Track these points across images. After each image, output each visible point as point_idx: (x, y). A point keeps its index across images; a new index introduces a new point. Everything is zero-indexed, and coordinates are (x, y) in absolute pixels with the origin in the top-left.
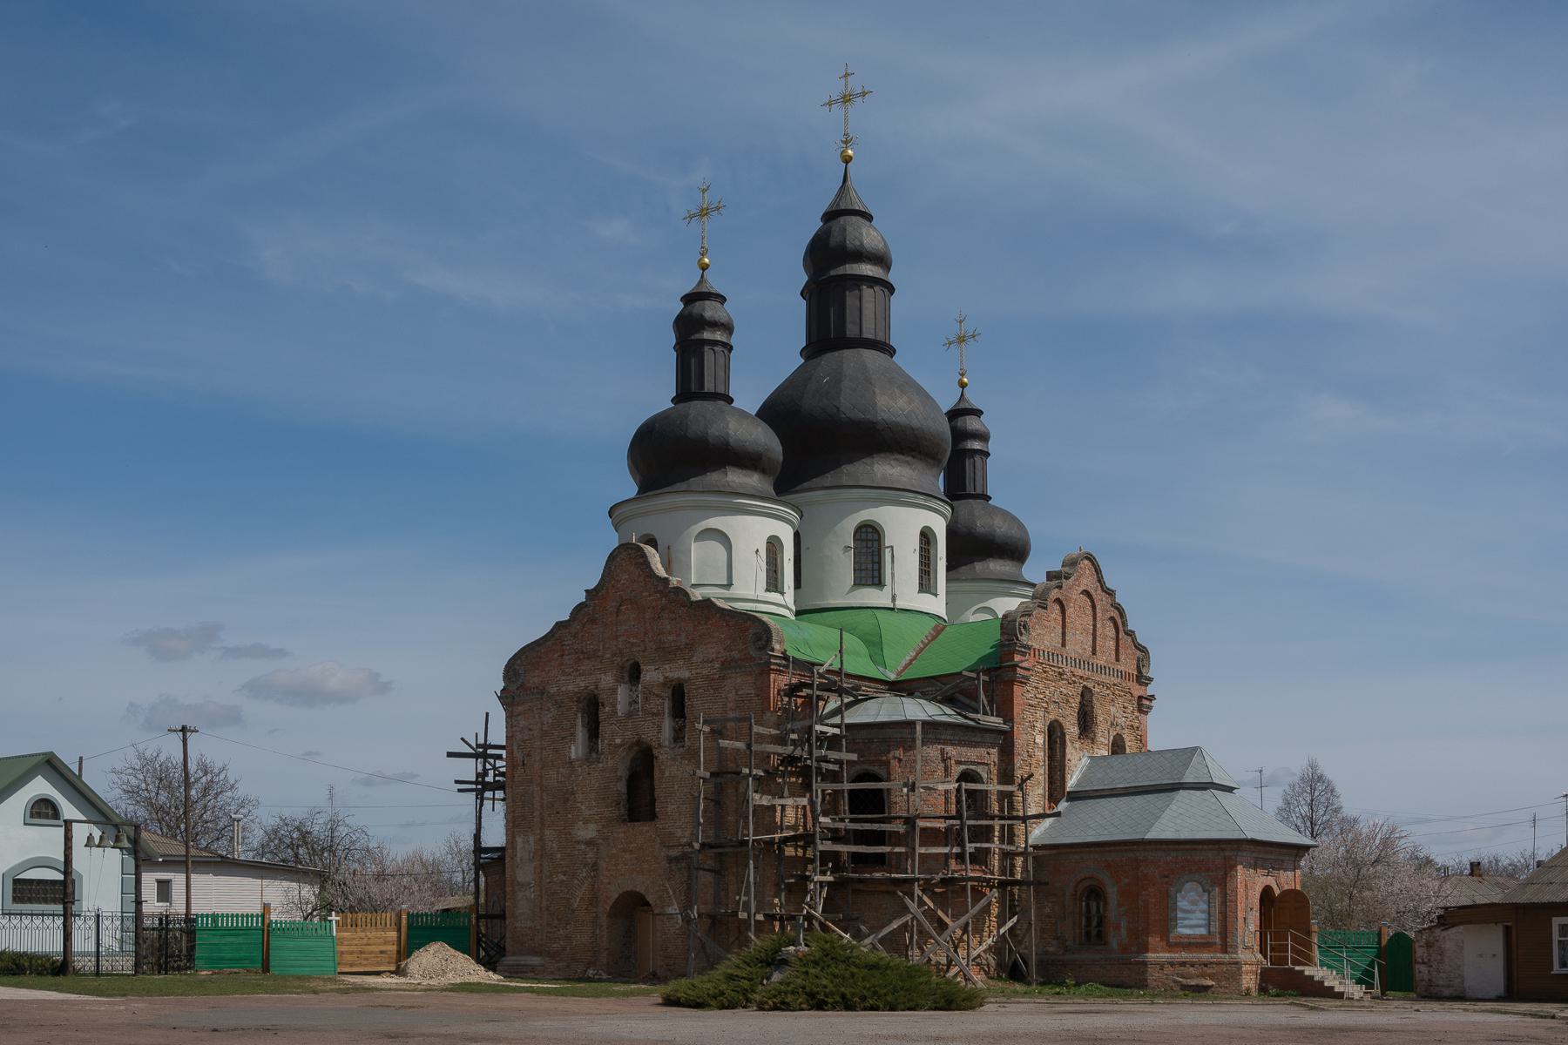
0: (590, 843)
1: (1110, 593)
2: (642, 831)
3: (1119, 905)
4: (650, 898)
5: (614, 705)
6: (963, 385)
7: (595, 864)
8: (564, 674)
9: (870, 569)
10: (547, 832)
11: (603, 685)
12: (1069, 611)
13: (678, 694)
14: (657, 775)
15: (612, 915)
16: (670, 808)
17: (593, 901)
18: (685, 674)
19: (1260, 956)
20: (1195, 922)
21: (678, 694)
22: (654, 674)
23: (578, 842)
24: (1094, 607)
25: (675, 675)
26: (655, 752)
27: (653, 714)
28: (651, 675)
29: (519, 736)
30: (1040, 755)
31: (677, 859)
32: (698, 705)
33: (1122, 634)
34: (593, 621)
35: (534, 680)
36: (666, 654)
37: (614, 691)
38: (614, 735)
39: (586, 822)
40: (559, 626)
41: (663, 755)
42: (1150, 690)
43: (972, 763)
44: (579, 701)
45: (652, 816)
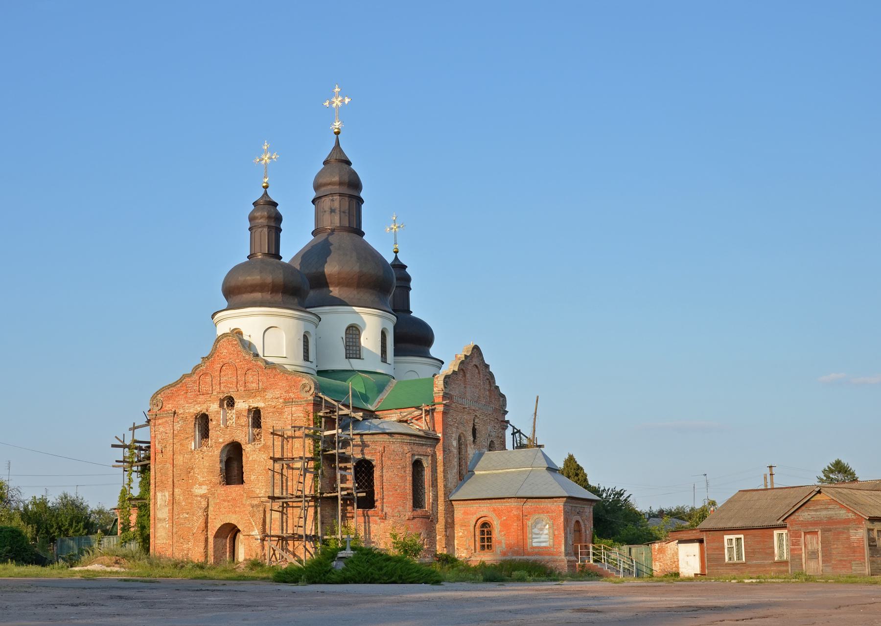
1: (487, 366)
3: (500, 531)
5: (218, 421)
6: (396, 252)
9: (353, 348)
10: (176, 490)
12: (468, 375)
13: (256, 416)
15: (216, 537)
16: (253, 477)
18: (260, 405)
19: (573, 558)
20: (541, 540)
21: (256, 416)
24: (479, 373)
26: (243, 447)
28: (241, 405)
29: (159, 437)
30: (455, 451)
31: (258, 506)
33: (493, 388)
34: (206, 374)
36: (250, 394)
37: (218, 413)
39: (201, 484)
41: (247, 449)
42: (507, 418)
43: (421, 455)
45: (242, 482)
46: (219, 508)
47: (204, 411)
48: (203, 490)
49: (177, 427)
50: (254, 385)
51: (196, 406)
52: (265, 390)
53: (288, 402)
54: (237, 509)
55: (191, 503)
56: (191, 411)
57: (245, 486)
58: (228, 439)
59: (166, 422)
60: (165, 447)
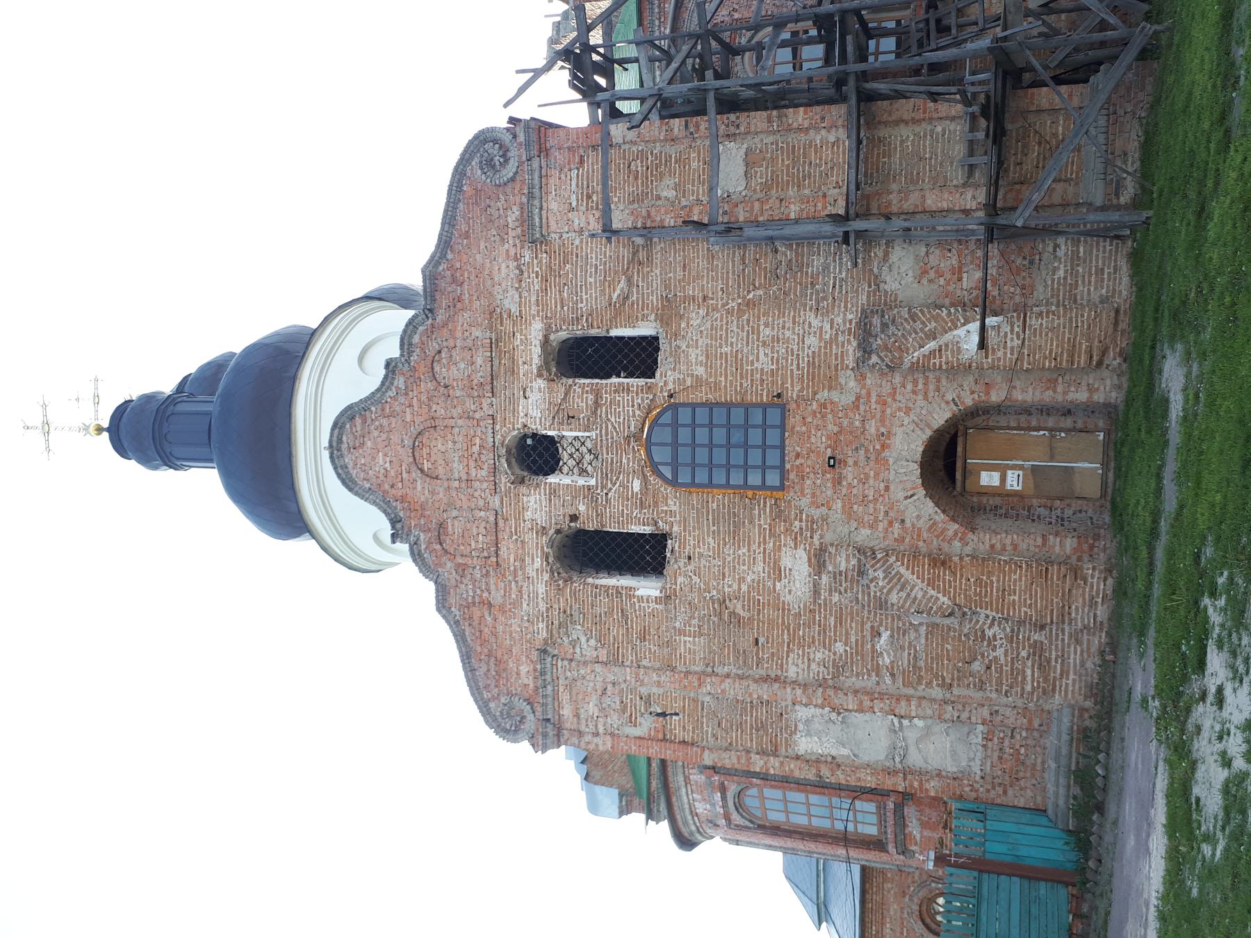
0: (819, 560)
2: (808, 439)
4: (940, 417)
5: (576, 492)
7: (860, 550)
8: (517, 604)
10: (792, 672)
11: (541, 519)
14: (702, 396)
16: (764, 361)
17: (940, 561)
18: (536, 329)
22: (534, 397)
23: (816, 592)
27: (597, 404)
28: (534, 406)
37: (553, 491)
39: (777, 572)
40: (443, 605)
44: (568, 580)
46: (864, 500)
48: (797, 562)
49: (588, 647)
52: (494, 315)
53: (534, 236)
54: (872, 428)
55: (840, 620)
56: (541, 589)
57: (793, 392)
59: (569, 687)
60: (648, 700)
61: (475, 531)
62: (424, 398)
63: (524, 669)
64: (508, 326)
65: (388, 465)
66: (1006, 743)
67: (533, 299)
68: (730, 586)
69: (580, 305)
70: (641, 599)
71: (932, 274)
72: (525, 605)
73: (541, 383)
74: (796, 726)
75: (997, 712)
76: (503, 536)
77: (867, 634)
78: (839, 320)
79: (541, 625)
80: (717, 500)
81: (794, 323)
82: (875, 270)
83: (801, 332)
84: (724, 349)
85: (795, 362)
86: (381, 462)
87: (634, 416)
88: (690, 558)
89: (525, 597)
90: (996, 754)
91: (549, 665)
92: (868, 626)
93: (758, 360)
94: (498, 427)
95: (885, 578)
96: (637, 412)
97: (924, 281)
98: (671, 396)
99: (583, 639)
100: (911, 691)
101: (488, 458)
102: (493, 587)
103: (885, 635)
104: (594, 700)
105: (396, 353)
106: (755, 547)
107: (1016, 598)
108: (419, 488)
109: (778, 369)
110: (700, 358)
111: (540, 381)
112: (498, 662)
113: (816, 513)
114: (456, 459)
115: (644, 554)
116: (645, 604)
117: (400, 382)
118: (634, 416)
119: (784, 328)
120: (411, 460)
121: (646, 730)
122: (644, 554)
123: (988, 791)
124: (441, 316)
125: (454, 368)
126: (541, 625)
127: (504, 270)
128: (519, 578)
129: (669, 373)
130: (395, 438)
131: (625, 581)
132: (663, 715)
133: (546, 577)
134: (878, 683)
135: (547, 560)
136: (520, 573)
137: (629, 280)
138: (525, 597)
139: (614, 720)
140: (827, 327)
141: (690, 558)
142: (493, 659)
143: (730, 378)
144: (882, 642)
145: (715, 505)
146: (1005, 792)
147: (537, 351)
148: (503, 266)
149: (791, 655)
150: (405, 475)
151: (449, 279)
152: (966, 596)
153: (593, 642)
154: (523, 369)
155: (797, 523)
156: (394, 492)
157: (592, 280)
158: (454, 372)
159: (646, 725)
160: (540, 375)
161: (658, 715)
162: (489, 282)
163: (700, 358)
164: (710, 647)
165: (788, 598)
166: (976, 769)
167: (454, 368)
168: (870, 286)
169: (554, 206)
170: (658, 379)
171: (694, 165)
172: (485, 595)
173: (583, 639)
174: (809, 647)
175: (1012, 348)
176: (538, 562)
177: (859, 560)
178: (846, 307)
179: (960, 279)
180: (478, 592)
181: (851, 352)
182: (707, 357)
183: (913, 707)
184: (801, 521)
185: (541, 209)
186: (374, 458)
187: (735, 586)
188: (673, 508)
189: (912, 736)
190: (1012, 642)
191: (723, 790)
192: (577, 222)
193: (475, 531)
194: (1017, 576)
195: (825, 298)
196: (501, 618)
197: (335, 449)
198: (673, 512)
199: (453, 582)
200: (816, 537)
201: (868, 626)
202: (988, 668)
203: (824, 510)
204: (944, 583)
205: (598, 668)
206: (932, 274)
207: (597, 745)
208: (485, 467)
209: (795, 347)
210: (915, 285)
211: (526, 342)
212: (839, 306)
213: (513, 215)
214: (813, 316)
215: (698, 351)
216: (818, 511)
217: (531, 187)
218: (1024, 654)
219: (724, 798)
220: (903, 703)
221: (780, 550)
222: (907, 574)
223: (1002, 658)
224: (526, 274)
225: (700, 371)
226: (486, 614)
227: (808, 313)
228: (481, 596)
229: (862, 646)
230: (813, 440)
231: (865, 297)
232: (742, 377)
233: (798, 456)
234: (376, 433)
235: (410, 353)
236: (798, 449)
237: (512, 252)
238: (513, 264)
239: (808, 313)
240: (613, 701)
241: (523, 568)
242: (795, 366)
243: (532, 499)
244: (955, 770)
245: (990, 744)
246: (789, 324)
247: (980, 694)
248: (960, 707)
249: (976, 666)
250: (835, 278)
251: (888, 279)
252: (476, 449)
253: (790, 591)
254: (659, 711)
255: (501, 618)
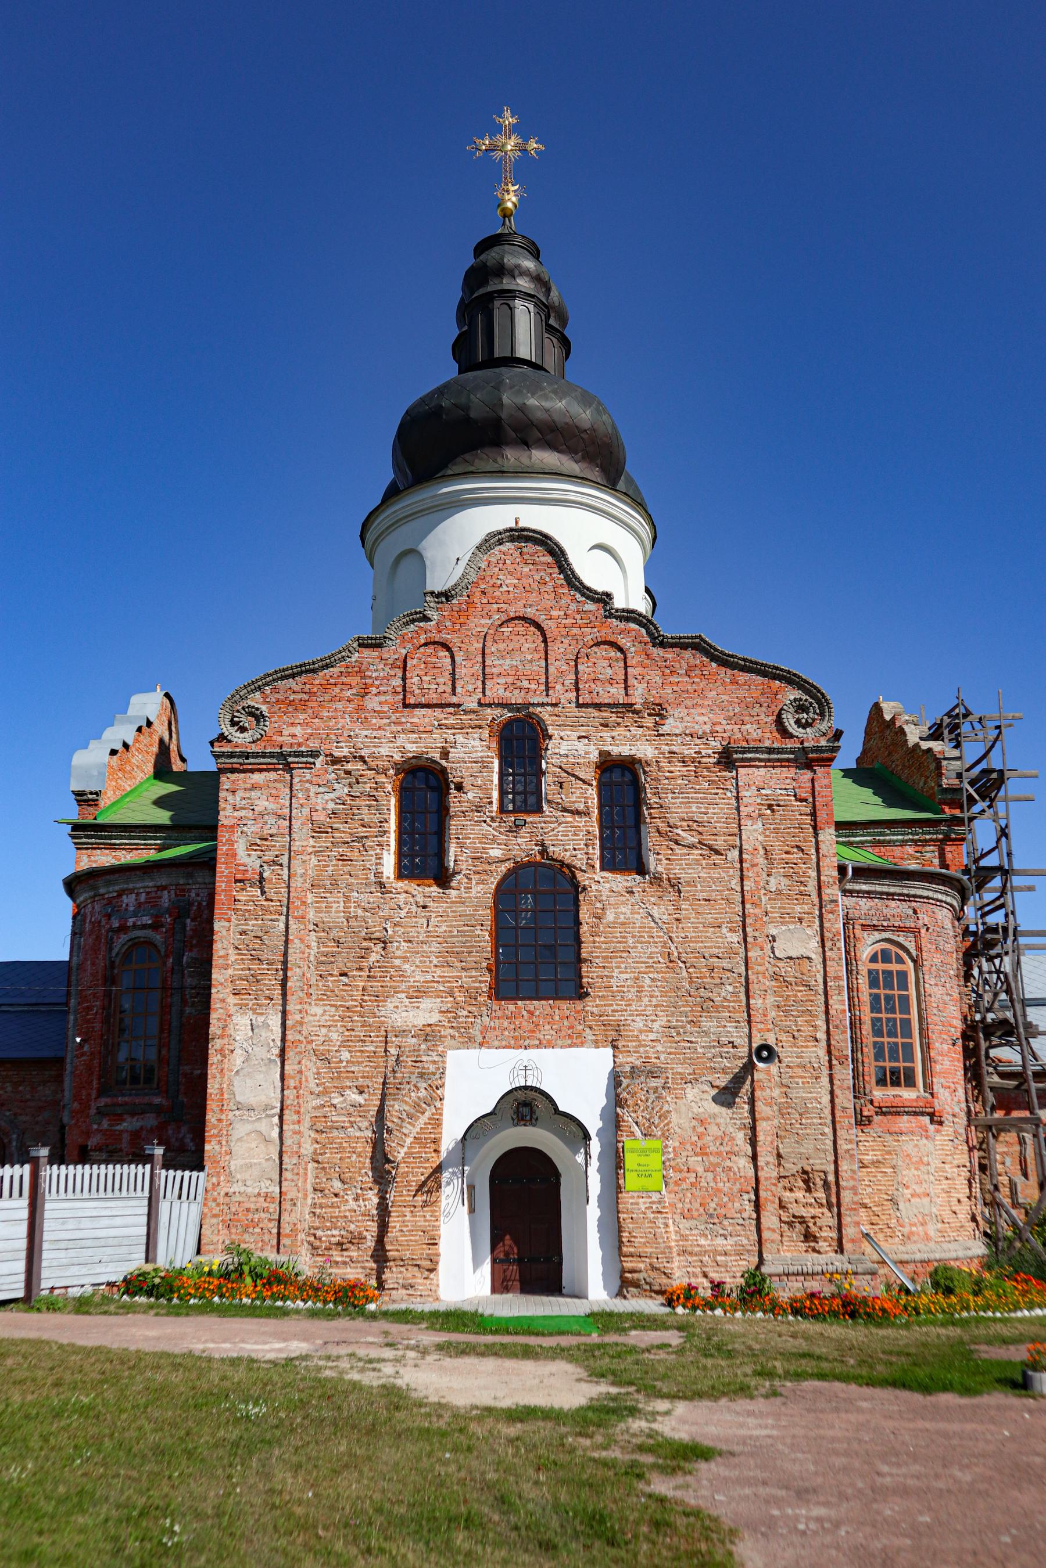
13: (622, 784)
16: (620, 977)
18: (645, 751)
21: (622, 784)
22: (581, 746)
23: (401, 1033)
25: (615, 750)
32: (679, 800)
35: (292, 732)
37: (485, 765)
38: (483, 843)
47: (436, 756)
48: (428, 1012)
49: (324, 801)
50: (616, 693)
51: (402, 739)
56: (384, 751)
57: (591, 1005)
58: (523, 846)
61: (441, 680)
62: (575, 630)
63: (297, 730)
64: (649, 722)
65: (505, 588)
66: (263, 1215)
67: (674, 749)
68: (398, 948)
69: (670, 795)
70: (379, 858)
71: (701, 1130)
72: (365, 733)
73: (594, 756)
74: (262, 1014)
75: (295, 1205)
76: (438, 712)
77: (361, 1082)
78: (659, 1048)
79: (346, 750)
80: (484, 936)
81: (655, 1006)
82: (704, 1078)
83: (647, 1013)
84: (631, 941)
85: (619, 1008)
86: (508, 582)
87: (566, 850)
88: (424, 907)
89: (375, 734)
90: (252, 1206)
91: (304, 760)
92: (368, 1082)
93: (621, 972)
94: (549, 708)
95: (419, 1098)
96: (568, 854)
97: (694, 1123)
98: (584, 889)
99: (332, 796)
100: (307, 1122)
101: (516, 697)
102: (383, 698)
103: (360, 1099)
104: (271, 806)
105: (619, 603)
106: (439, 972)
107: (407, 1218)
108: (483, 621)
109: (613, 992)
110: (622, 916)
111: (596, 753)
112: (304, 703)
113: (476, 1032)
114: (514, 663)
115: (425, 856)
116: (374, 861)
117: (590, 606)
118: (566, 850)
119: (652, 996)
120: (512, 615)
121: (245, 860)
122: (425, 856)
123: (215, 1200)
124: (657, 652)
125: (606, 663)
126: (346, 750)
127: (701, 721)
128: (394, 728)
129: (607, 885)
130: (533, 597)
131: (392, 839)
132: (262, 880)
133: (397, 757)
134: (312, 1093)
135: (414, 757)
136: (399, 728)
137: (691, 847)
138: (375, 734)
139: (252, 828)
140: (652, 1036)
141: (424, 907)
142: (306, 697)
143: (603, 946)
144: (353, 1096)
145: (478, 932)
146: (215, 1216)
147: (621, 750)
148: (706, 719)
149: (333, 1009)
150: (495, 606)
151: (692, 662)
152: (407, 1173)
153: (331, 805)
154: (606, 735)
155: (466, 1013)
156: (478, 594)
157: (694, 809)
158: (602, 665)
159: (250, 861)
160: (601, 753)
161: (261, 874)
162: (689, 703)
163: (622, 916)
164: (336, 927)
165: (390, 1005)
166: (236, 1188)
167: (606, 663)
168: (689, 1074)
169: (763, 771)
170: (599, 875)
171: (798, 908)
172: (374, 690)
173: (332, 796)
174: (342, 1026)
175: (637, 1204)
176: (412, 748)
177: (434, 1074)
178: (670, 1053)
179: (696, 1155)
180: (377, 683)
181: (629, 1059)
182: (623, 924)
183: (292, 1127)
184: (467, 1017)
185: (760, 760)
186: (511, 573)
187: (398, 953)
188: (474, 890)
189: (263, 1126)
190: (362, 1215)
191: (155, 926)
192: (747, 794)
193: (441, 680)
194: (428, 1218)
195: (678, 1034)
196: (350, 707)
197: (520, 535)
198: (474, 894)
199: (385, 656)
200: (451, 1031)
201: (368, 1082)
202: (336, 1195)
203: (479, 1039)
204: (418, 1152)
205: (306, 811)
206: (701, 1130)
207: (224, 809)
208: (508, 694)
209: (634, 1007)
210: (691, 1115)
211: (634, 740)
212: (671, 1047)
213: (752, 730)
214: (663, 1023)
215: (629, 915)
216: (477, 1033)
217: (779, 751)
218: (352, 1227)
219: (144, 927)
220: (295, 1117)
221: (438, 997)
222: (423, 1119)
223: (347, 1208)
224: (698, 741)
225: (610, 916)
226: (354, 691)
227: (665, 1019)
228: (372, 685)
229: (347, 1078)
230: (547, 1027)
231: (679, 1070)
232: (604, 958)
233: (531, 1013)
234: (537, 577)
235: (620, 618)
236: (537, 1013)
237: (718, 728)
238: (707, 728)
239: (665, 1019)
240: (272, 826)
241: (403, 731)
242: (615, 1007)
243: (477, 743)
244: (233, 1168)
245: (262, 1199)
246: (654, 1001)
247: (310, 1189)
248: (296, 1171)
249: (337, 1185)
250: (697, 1042)
251: (696, 1090)
252: (525, 684)
253: (397, 1007)
254: (265, 875)
255: (350, 707)
